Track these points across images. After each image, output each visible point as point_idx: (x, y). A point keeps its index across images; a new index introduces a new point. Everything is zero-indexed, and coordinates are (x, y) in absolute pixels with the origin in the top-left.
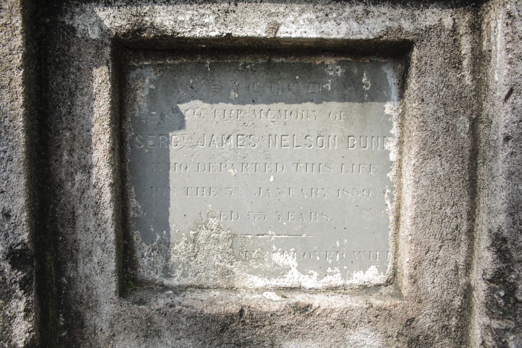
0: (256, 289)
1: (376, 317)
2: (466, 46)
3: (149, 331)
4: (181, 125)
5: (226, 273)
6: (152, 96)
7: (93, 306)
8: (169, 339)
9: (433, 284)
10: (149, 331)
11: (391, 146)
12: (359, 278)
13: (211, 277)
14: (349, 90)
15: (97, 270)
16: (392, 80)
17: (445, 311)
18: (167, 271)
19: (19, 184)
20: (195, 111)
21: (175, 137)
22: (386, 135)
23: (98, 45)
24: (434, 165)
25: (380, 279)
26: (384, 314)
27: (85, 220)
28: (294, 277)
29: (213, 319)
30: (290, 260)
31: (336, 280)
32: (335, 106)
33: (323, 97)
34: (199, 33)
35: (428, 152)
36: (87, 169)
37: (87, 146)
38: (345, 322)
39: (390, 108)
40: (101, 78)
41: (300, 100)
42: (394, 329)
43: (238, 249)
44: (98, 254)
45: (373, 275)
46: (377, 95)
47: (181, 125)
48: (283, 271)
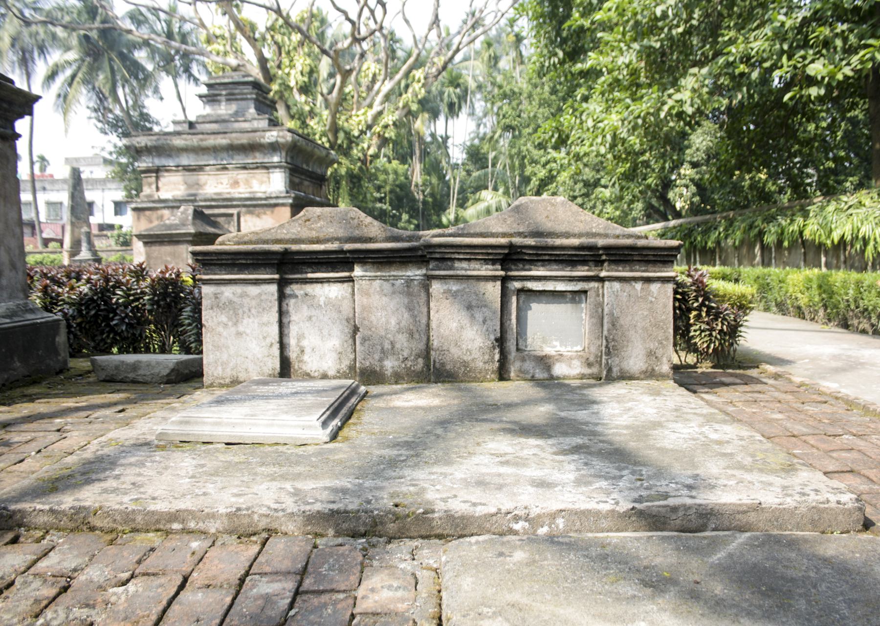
0: (548, 350)
1: (579, 357)
2: (601, 292)
3: (523, 360)
4: (531, 309)
5: (541, 347)
6: (524, 302)
7: (510, 354)
8: (528, 362)
9: (593, 349)
10: (523, 360)
11: (583, 315)
12: (575, 349)
13: (537, 348)
14: (573, 301)
15: (511, 345)
16: (584, 298)
17: (596, 356)
18: (526, 346)
19: (499, 323)
20: (534, 306)
21: (529, 312)
22: (582, 312)
23: (514, 291)
24: (593, 320)
25: (581, 349)
26: (582, 357)
27: (509, 332)
28: (558, 348)
29: (539, 357)
30: (557, 343)
31: (569, 349)
32: (569, 305)
33: (567, 303)
34: (538, 289)
35: (591, 317)
36: (510, 320)
37: (511, 315)
38: (571, 358)
39: (583, 305)
40: (514, 299)
41: (560, 303)
42: (584, 361)
43: (544, 341)
44: (512, 341)
45: (579, 348)
46: (580, 302)
47: (531, 309)
48: (555, 347)
